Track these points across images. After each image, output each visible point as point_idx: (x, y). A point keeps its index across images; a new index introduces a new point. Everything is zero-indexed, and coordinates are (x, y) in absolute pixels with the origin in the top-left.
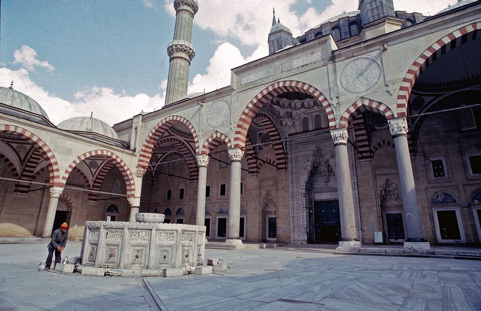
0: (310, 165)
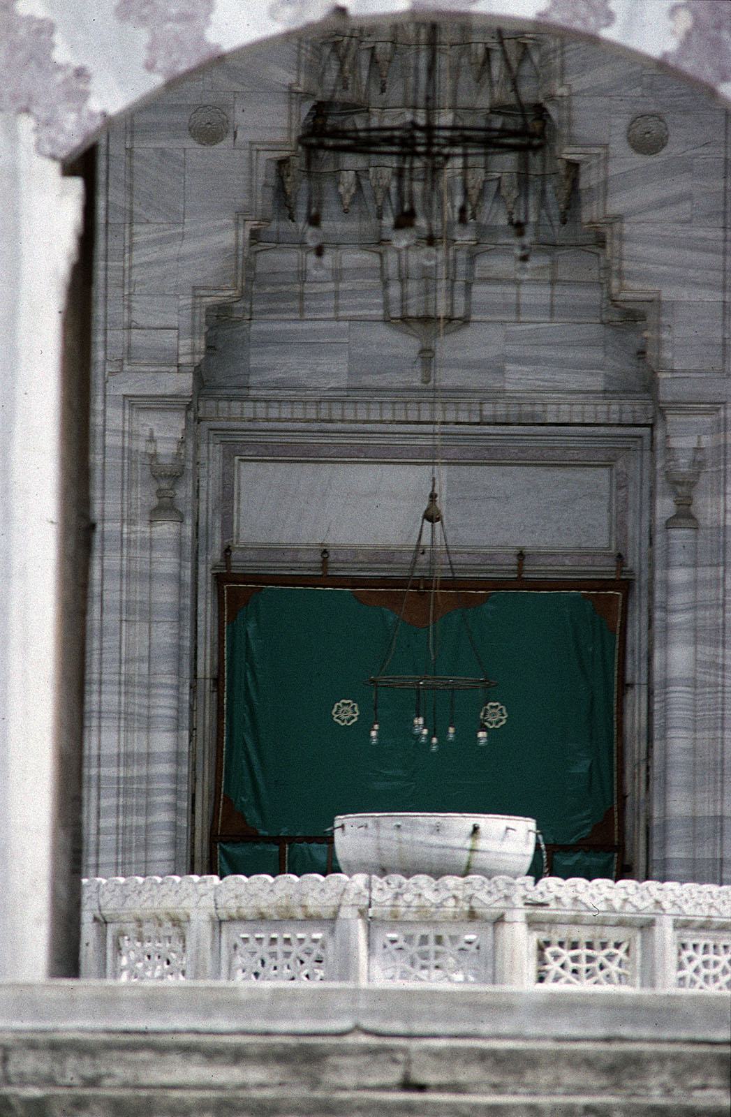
0: (290, 78)
